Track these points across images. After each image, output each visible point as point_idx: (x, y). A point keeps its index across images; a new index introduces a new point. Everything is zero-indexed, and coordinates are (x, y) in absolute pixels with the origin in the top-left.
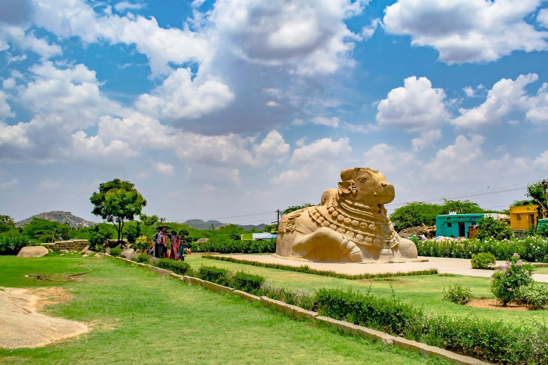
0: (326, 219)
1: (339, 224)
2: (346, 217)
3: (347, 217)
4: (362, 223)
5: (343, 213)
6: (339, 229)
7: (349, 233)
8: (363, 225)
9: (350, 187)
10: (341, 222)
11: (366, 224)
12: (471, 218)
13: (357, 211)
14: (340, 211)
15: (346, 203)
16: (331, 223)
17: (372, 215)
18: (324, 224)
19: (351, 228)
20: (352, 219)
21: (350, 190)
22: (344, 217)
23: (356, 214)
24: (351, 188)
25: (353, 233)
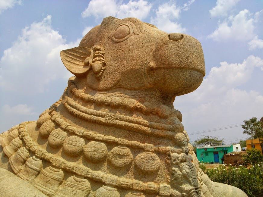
0: (24, 144)
1: (49, 155)
2: (71, 133)
3: (73, 133)
4: (116, 149)
5: (65, 122)
6: (48, 171)
7: (74, 183)
8: (121, 156)
9: (90, 59)
10: (55, 148)
11: (127, 150)
12: (223, 148)
13: (102, 116)
14: (58, 117)
15: (77, 98)
16: (32, 153)
17: (145, 125)
18: (15, 156)
19: (82, 166)
20: (88, 139)
21: (87, 64)
22: (65, 133)
23: (100, 123)
24: (91, 61)
25: (87, 183)
